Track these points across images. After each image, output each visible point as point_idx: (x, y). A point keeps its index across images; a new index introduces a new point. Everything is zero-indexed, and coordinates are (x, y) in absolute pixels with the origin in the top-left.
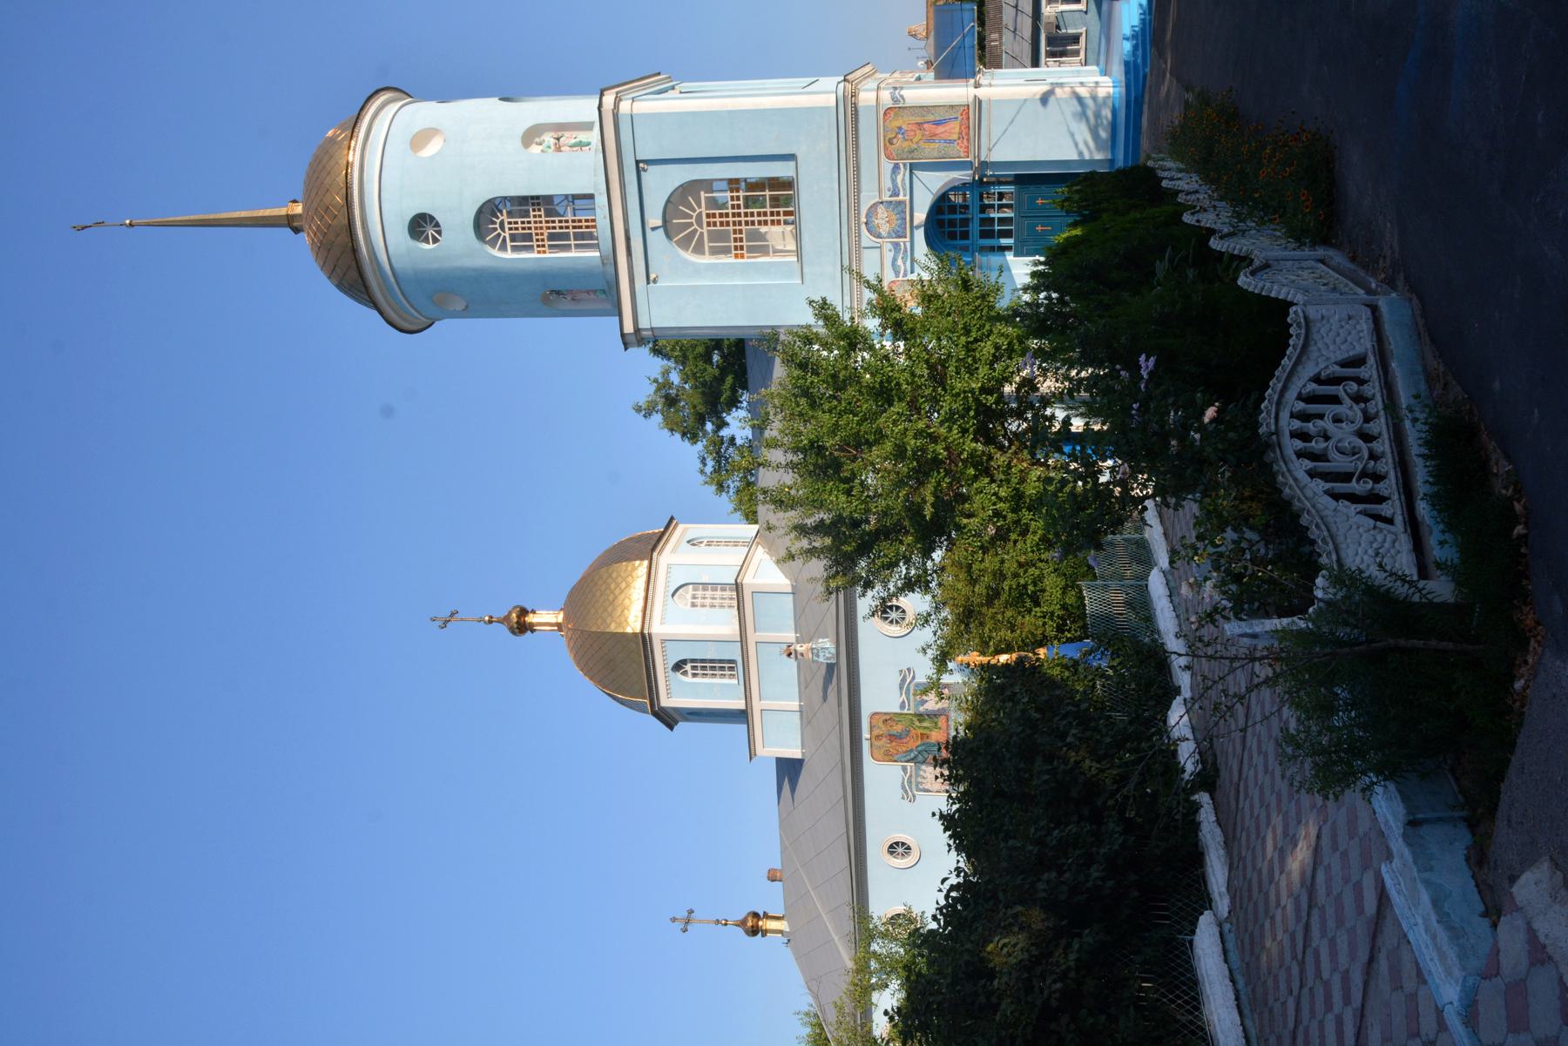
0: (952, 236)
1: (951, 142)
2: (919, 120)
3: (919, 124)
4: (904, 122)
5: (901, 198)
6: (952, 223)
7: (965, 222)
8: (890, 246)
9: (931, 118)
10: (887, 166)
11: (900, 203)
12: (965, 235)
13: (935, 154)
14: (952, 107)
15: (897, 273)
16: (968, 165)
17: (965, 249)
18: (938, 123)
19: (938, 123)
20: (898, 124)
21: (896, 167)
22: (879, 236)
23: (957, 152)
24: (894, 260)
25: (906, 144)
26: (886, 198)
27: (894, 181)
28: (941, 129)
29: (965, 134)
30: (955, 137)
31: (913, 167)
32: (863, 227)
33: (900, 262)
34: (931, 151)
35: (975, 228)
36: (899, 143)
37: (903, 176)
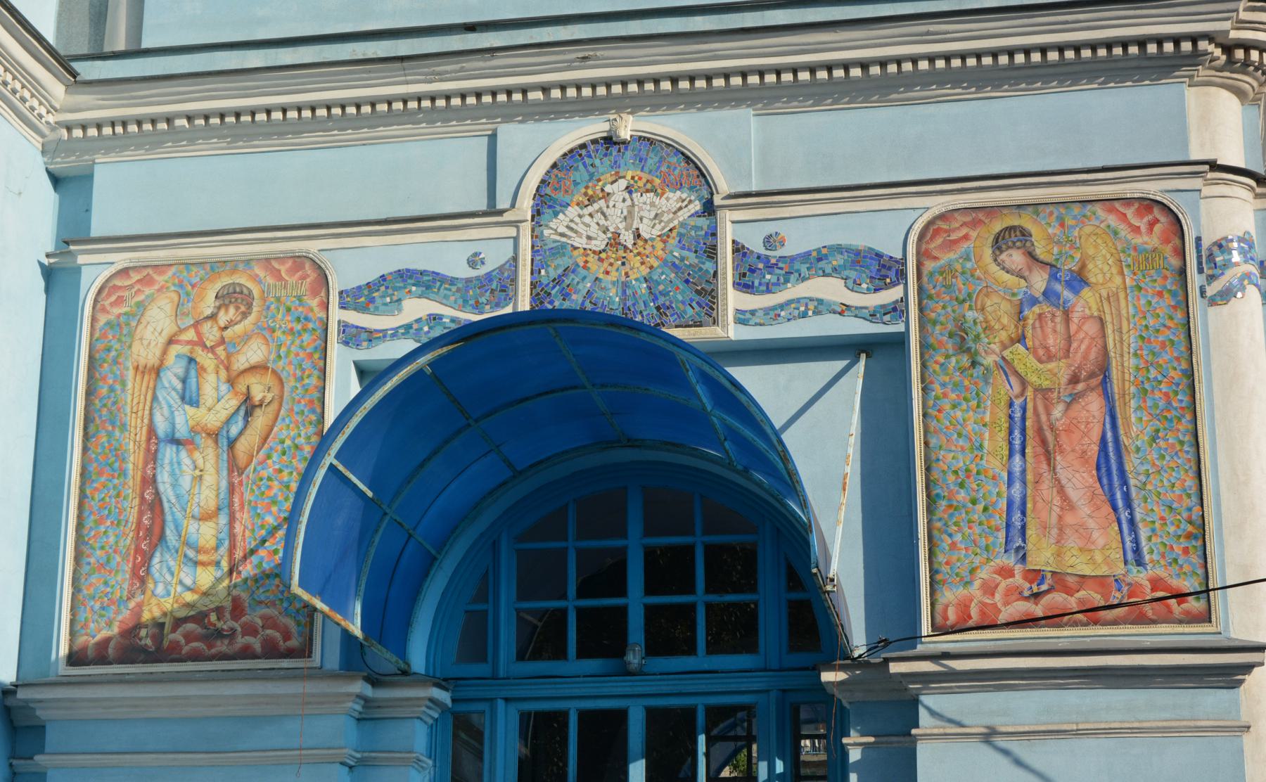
0: (538, 576)
1: (1016, 537)
2: (1124, 368)
3: (1103, 370)
4: (1113, 300)
5: (733, 300)
6: (606, 577)
7: (604, 637)
8: (495, 257)
9: (1136, 428)
10: (888, 228)
11: (708, 299)
12: (542, 640)
13: (953, 458)
14: (1199, 532)
15: (351, 299)
16: (897, 628)
17: (474, 639)
18: (1109, 464)
19: (1109, 464)
20: (1101, 269)
21: (884, 270)
22: (545, 203)
23: (965, 570)
24: (427, 282)
25: (1000, 311)
26: (731, 228)
27: (816, 261)
28: (1079, 480)
29: (1051, 601)
30: (1042, 556)
31: (881, 352)
32: (594, 127)
33: (416, 308)
34: (963, 436)
35: (577, 686)
36: (1004, 279)
37: (841, 307)
